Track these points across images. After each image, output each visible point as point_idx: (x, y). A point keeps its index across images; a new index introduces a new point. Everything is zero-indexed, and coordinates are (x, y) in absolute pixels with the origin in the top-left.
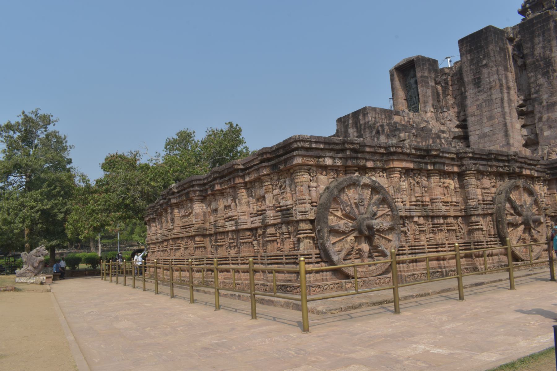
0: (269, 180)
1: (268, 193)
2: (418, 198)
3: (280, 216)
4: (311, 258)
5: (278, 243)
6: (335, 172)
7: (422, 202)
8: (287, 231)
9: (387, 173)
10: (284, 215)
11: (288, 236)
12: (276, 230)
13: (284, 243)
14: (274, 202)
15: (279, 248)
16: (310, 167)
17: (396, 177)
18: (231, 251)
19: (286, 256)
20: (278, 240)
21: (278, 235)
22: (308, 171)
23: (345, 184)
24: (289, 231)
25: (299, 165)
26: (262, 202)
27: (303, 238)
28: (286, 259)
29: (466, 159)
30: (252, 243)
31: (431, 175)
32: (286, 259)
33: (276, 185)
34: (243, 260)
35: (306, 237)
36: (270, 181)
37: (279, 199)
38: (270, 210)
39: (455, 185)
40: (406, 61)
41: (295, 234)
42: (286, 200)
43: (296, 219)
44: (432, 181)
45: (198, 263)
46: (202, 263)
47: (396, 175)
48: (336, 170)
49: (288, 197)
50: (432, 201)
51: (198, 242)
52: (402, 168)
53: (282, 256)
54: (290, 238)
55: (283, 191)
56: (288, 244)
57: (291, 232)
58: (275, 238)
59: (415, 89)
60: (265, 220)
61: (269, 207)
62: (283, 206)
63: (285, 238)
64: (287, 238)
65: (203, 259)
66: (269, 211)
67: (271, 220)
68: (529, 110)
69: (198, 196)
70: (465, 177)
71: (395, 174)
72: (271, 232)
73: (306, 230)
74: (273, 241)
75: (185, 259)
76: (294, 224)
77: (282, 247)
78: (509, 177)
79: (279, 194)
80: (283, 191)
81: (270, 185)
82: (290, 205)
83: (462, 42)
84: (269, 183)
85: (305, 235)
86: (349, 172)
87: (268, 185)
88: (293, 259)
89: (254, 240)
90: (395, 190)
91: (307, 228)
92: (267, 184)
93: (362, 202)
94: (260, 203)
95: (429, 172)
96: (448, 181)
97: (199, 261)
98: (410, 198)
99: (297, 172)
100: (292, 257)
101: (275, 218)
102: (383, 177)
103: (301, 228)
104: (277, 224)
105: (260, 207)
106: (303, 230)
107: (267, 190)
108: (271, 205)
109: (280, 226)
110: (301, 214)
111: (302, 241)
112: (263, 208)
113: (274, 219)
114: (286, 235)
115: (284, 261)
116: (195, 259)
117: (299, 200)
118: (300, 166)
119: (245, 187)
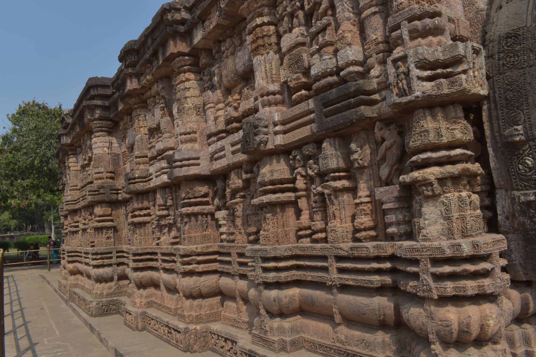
0: (266, 10)
1: (261, 49)
3: (311, 112)
4: (486, 274)
5: (298, 213)
8: (342, 164)
10: (326, 105)
11: (345, 183)
12: (293, 169)
13: (332, 209)
14: (284, 74)
15: (306, 229)
18: (163, 238)
19: (339, 259)
20: (303, 203)
21: (300, 183)
24: (350, 163)
26: (240, 93)
27: (441, 181)
28: (341, 271)
30: (212, 215)
32: (341, 271)
33: (292, 15)
34: (189, 263)
35: (455, 179)
36: (269, 14)
37: (305, 56)
38: (270, 104)
41: (384, 171)
42: (336, 51)
43: (404, 100)
45: (100, 262)
46: (107, 261)
49: (348, 35)
51: (100, 216)
53: (324, 258)
54: (353, 191)
55: (324, 21)
56: (348, 212)
57: (362, 168)
58: (290, 196)
60: (256, 135)
61: (268, 94)
62: (324, 75)
63: (337, 191)
64: (345, 190)
65: (111, 253)
66: (267, 109)
67: (276, 133)
69: (99, 119)
72: (276, 176)
73: (451, 146)
74: (283, 205)
75: (83, 251)
76: (378, 134)
77: (319, 225)
79: (303, 44)
80: (324, 21)
81: (269, 24)
82: (355, 63)
84: (266, 19)
85: (450, 169)
87: (263, 24)
88: (379, 272)
89: (219, 209)
91: (458, 135)
92: (259, 21)
94: (236, 97)
97: (102, 259)
100: (375, 265)
101: (288, 126)
103: (432, 138)
104: (299, 145)
105: (236, 109)
106: (436, 148)
107: (260, 42)
108: (274, 87)
109: (309, 149)
111: (435, 197)
112: (246, 105)
113: (285, 132)
114: (340, 178)
115: (334, 276)
116: (93, 254)
117: (410, 20)
119: (194, 68)
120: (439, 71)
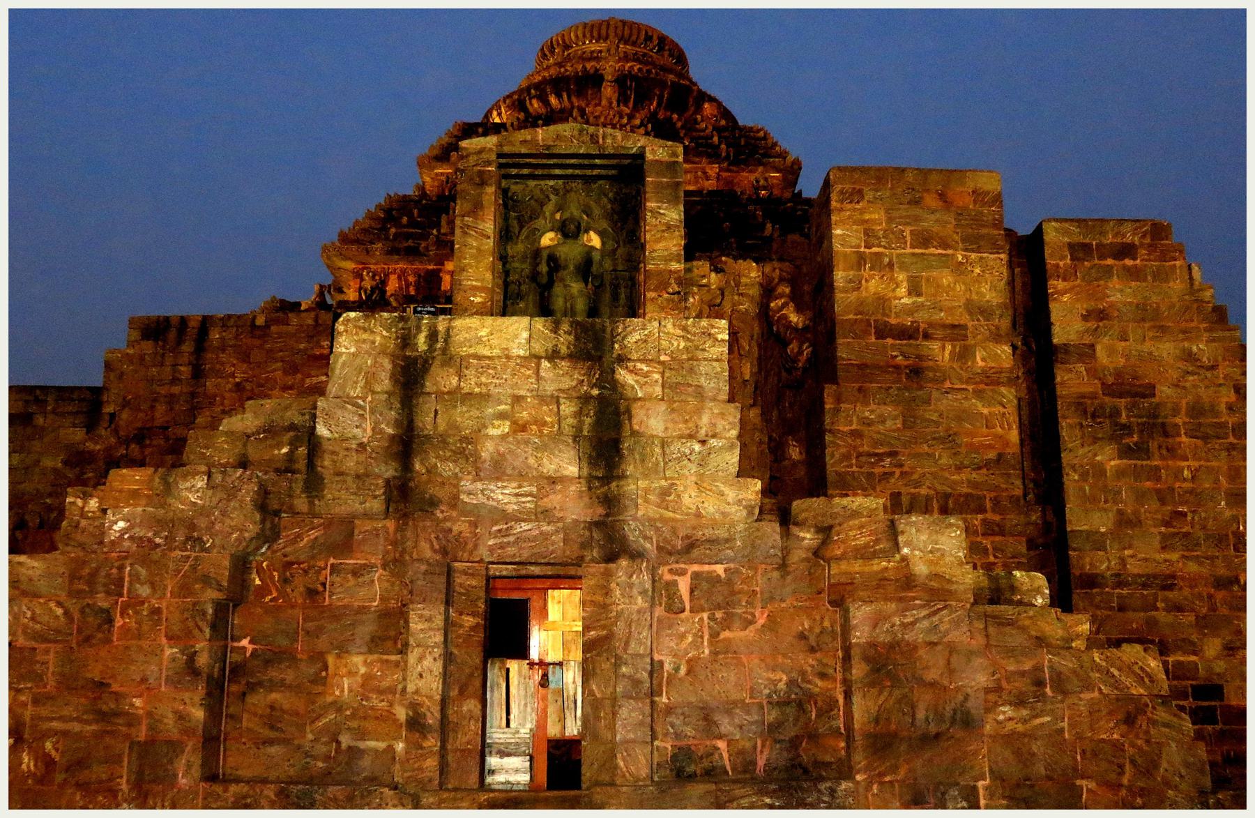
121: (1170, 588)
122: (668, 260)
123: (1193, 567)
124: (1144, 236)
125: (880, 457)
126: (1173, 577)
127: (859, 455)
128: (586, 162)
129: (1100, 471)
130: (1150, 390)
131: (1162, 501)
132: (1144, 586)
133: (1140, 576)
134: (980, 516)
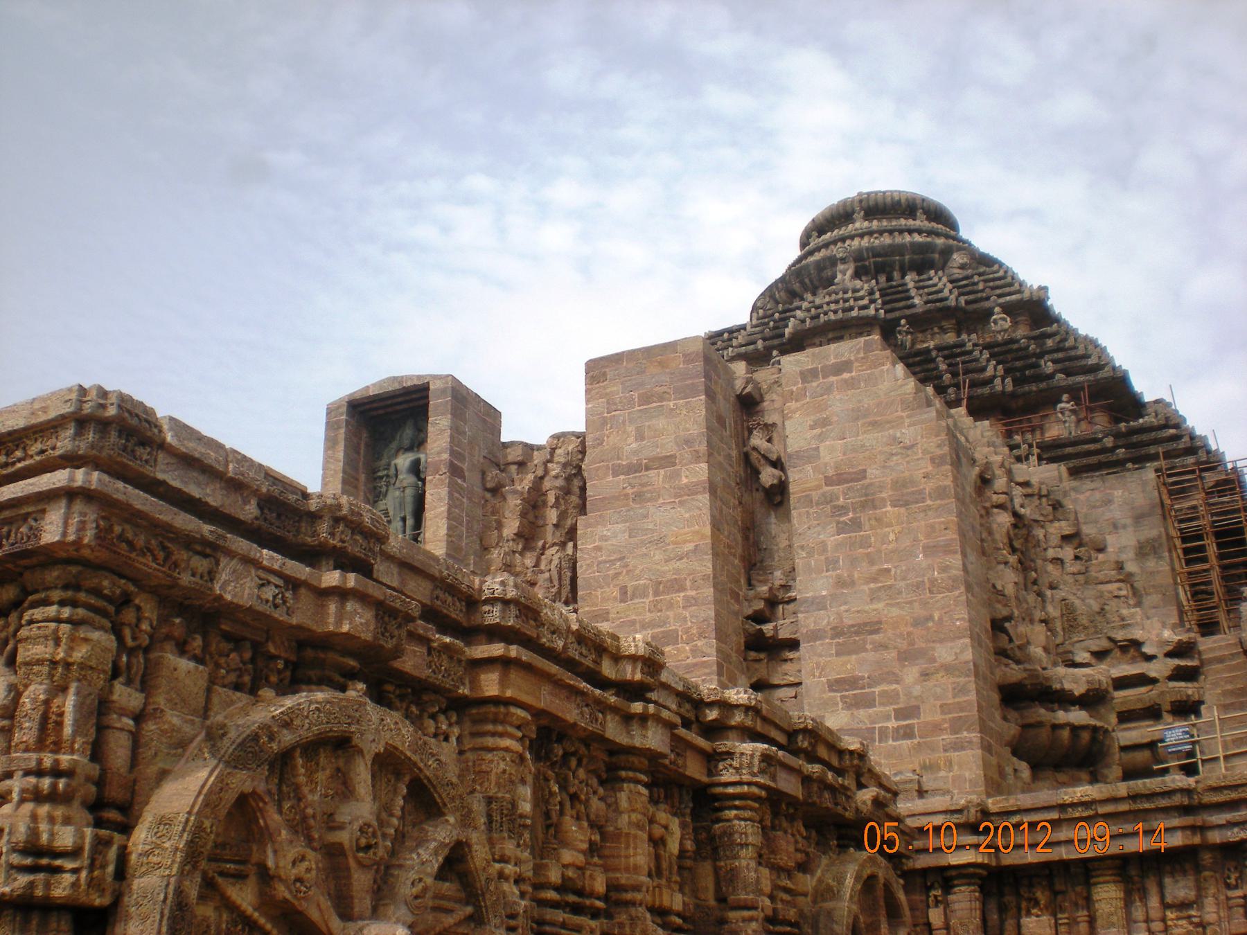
2: (570, 873)
6: (248, 655)
7: (580, 893)
9: (468, 725)
16: (132, 588)
17: (507, 749)
22: (111, 609)
23: (305, 731)
25: (69, 561)
29: (732, 734)
31: (623, 774)
39: (682, 839)
40: (397, 386)
44: (624, 804)
47: (507, 742)
48: (256, 646)
50: (614, 895)
52: (538, 713)
59: (409, 492)
68: (784, 634)
70: (721, 809)
71: (501, 735)
78: (838, 839)
83: (597, 371)
86: (313, 674)
90: (497, 817)
93: (368, 847)
95: (614, 759)
96: (663, 816)
98: (538, 869)
99: (46, 603)
102: (446, 739)
110: (28, 861)
118: (74, 569)
120: (44, 861)
121: (876, 631)
122: (439, 453)
123: (895, 612)
124: (858, 352)
125: (613, 562)
126: (880, 622)
127: (600, 563)
128: (407, 398)
129: (823, 547)
130: (862, 474)
131: (872, 563)
132: (857, 633)
133: (853, 626)
134: (682, 594)
